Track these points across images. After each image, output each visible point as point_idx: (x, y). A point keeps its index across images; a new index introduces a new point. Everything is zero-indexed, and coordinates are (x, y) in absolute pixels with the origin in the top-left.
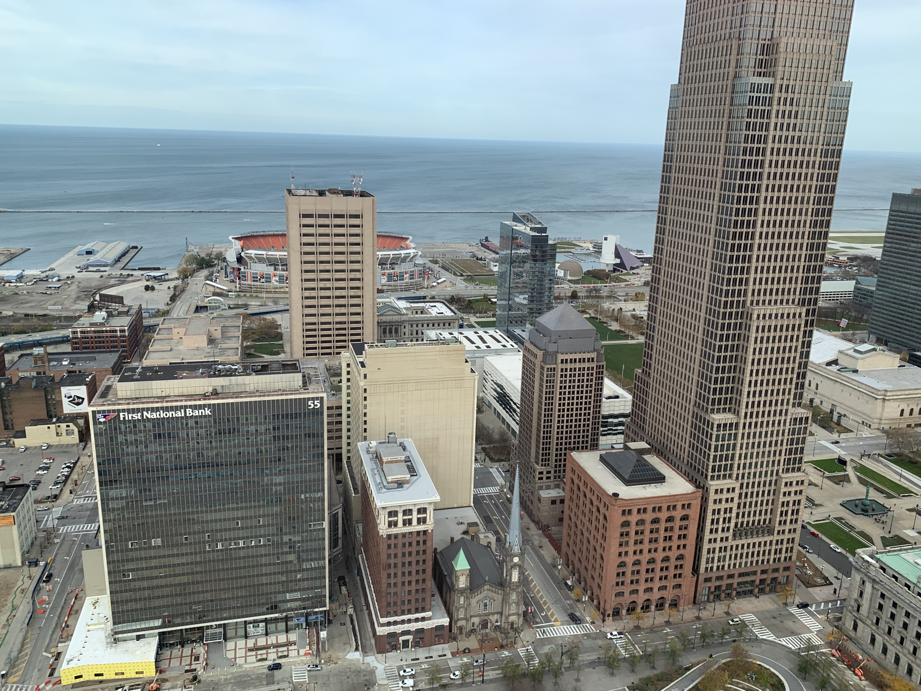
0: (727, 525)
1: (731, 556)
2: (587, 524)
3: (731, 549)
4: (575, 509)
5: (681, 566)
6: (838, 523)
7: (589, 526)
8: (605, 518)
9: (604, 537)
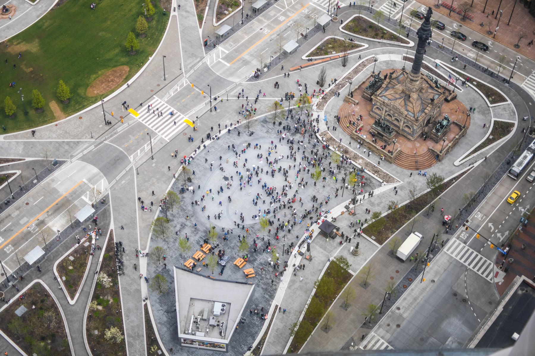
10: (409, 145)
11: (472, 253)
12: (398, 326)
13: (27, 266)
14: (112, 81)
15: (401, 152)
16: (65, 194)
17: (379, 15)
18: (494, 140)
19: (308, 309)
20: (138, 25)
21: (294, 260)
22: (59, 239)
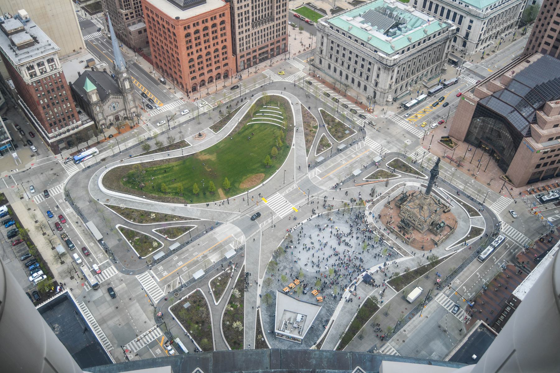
0: (248, 21)
1: (252, 39)
2: (164, 41)
3: (252, 36)
5: (226, 53)
6: (308, 7)
7: (166, 42)
8: (174, 34)
9: (176, 47)
10: (420, 235)
11: (452, 303)
12: (404, 341)
13: (194, 280)
14: (255, 181)
15: (415, 239)
16: (220, 242)
18: (470, 238)
19: (351, 325)
20: (272, 152)
21: (347, 294)
22: (214, 267)
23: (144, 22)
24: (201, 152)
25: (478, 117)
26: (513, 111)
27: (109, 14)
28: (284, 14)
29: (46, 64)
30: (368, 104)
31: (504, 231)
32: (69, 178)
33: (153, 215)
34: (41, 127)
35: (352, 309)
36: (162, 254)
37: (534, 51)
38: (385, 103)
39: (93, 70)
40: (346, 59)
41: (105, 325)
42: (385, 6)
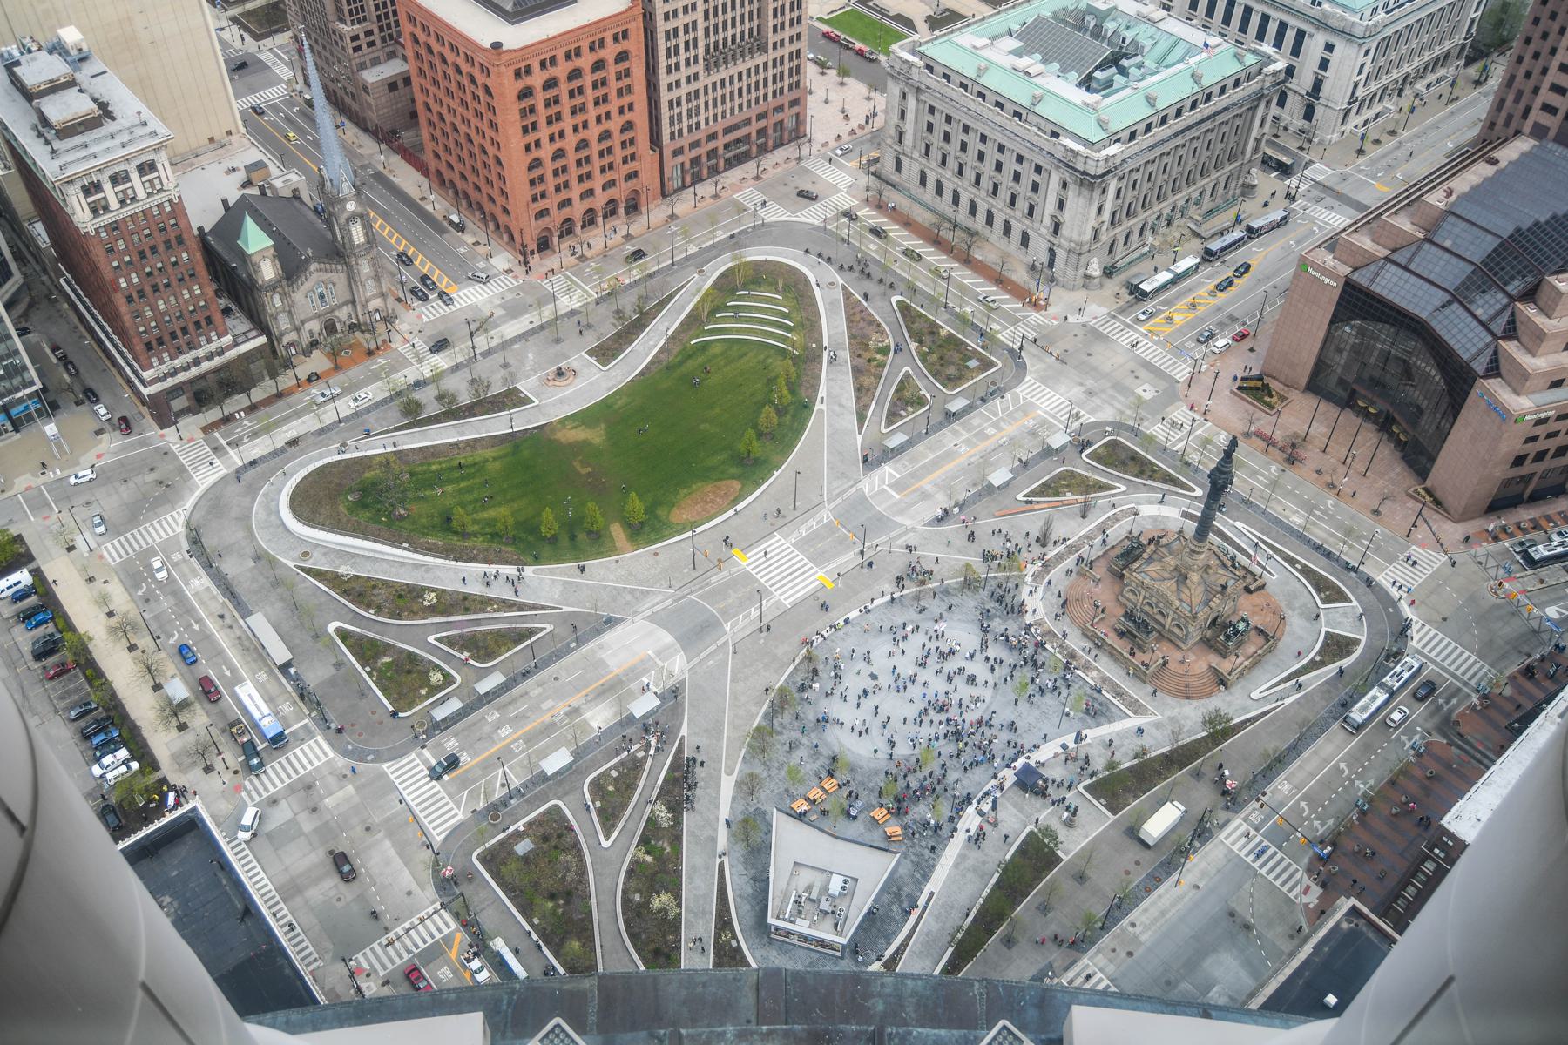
0: (693, 53)
1: (706, 103)
2: (460, 110)
3: (706, 93)
4: (432, 89)
5: (632, 141)
7: (465, 112)
8: (488, 92)
9: (494, 126)
12: (1130, 954)
13: (543, 778)
14: (712, 501)
16: (617, 671)
17: (1150, 440)
18: (1322, 664)
20: (762, 419)
21: (970, 820)
22: (598, 741)
23: (405, 58)
24: (562, 421)
25: (1347, 321)
26: (1449, 303)
27: (308, 36)
28: (794, 31)
29: (135, 176)
30: (1032, 285)
31: (1419, 646)
32: (198, 493)
33: (431, 597)
34: (121, 353)
35: (984, 863)
36: (455, 705)
37: (1511, 130)
38: (1080, 281)
39: (263, 193)
40: (970, 158)
41: (298, 900)
42: (1082, 6)
